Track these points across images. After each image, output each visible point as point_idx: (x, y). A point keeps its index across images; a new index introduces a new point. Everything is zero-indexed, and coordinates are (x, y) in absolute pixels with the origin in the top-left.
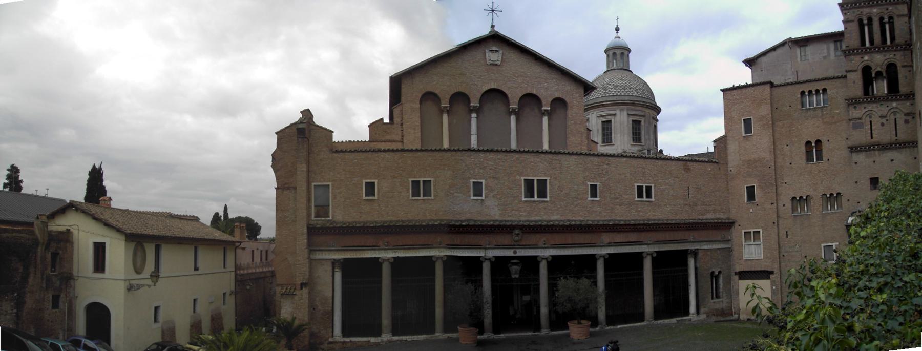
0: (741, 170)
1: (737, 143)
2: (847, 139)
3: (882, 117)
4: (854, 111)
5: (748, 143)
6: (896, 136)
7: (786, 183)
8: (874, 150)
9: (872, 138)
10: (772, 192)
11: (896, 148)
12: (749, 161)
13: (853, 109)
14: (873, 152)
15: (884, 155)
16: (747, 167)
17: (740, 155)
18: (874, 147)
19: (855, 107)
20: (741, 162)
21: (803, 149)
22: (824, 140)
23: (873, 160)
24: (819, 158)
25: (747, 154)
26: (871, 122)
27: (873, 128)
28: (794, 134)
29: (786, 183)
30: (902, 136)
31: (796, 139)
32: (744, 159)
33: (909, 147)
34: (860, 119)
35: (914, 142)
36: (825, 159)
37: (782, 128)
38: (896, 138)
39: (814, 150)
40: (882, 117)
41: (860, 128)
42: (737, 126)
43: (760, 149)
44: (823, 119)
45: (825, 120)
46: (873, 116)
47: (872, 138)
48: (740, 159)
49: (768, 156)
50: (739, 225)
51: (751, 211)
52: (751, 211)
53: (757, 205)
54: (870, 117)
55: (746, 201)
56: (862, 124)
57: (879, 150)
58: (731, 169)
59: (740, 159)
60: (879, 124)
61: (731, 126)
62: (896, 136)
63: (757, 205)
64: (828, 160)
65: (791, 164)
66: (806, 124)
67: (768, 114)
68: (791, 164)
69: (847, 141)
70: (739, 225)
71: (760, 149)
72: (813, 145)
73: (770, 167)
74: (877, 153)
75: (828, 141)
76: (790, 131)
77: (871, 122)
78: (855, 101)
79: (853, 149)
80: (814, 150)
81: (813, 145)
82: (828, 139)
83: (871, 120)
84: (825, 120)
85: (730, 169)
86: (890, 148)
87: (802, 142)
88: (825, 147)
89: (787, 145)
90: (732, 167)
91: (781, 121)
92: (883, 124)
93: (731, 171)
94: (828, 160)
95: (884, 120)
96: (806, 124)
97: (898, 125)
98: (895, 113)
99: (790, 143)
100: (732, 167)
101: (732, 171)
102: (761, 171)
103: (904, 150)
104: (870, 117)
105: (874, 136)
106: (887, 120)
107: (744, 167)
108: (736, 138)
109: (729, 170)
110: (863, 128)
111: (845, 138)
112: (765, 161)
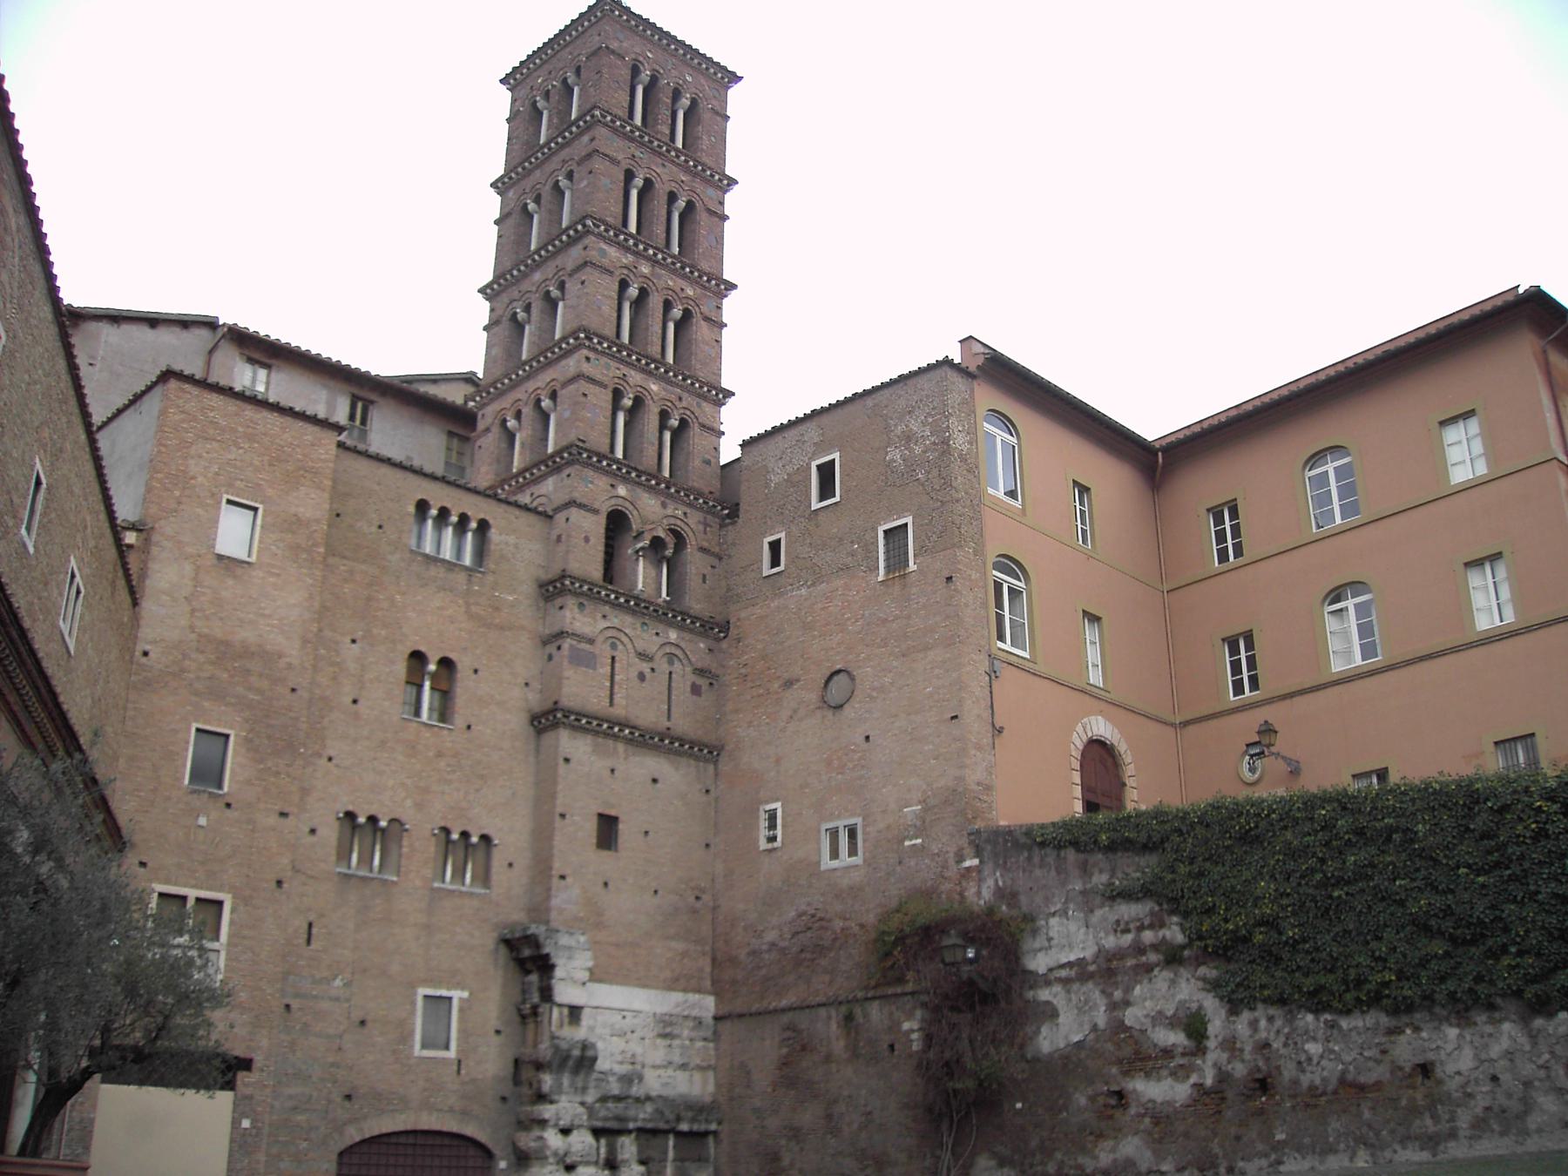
0: (187, 663)
1: (188, 568)
2: (527, 684)
3: (643, 656)
4: (577, 616)
5: (230, 582)
6: (669, 718)
7: (330, 759)
8: (615, 737)
9: (611, 703)
10: (289, 776)
11: (669, 752)
12: (227, 644)
13: (576, 610)
14: (610, 742)
15: (637, 759)
16: (213, 663)
17: (193, 611)
18: (620, 730)
19: (581, 605)
20: (193, 636)
21: (401, 668)
22: (463, 663)
23: (609, 763)
24: (444, 712)
25: (221, 619)
26: (613, 658)
27: (617, 678)
28: (379, 613)
29: (330, 759)
30: (682, 724)
31: (383, 632)
32: (206, 630)
33: (697, 759)
34: (591, 641)
35: (715, 747)
36: (459, 721)
37: (346, 580)
38: (668, 724)
39: (427, 684)
40: (643, 656)
41: (586, 667)
42: (200, 511)
43: (270, 616)
44: (468, 604)
45: (474, 609)
46: (620, 647)
47: (611, 703)
48: (192, 628)
49: (294, 652)
50: (143, 864)
51: (202, 821)
52: (202, 821)
53: (228, 805)
54: (614, 646)
55: (186, 782)
56: (594, 656)
57: (629, 741)
58: (147, 648)
59: (192, 628)
60: (634, 674)
61: (179, 503)
62: (669, 718)
63: (228, 805)
64: (469, 727)
65: (355, 702)
66: (419, 598)
67: (318, 521)
68: (355, 702)
69: (526, 689)
70: (143, 864)
71: (270, 616)
72: (432, 667)
73: (293, 690)
74: (621, 747)
75: (476, 671)
76: (369, 599)
77: (613, 658)
78: (590, 589)
79: (567, 717)
80: (427, 684)
81: (432, 667)
82: (477, 667)
83: (615, 654)
84: (474, 609)
85: (141, 647)
86: (655, 748)
87: (399, 647)
88: (465, 685)
89: (354, 641)
90: (154, 642)
91: (344, 557)
92: (642, 677)
93: (146, 654)
94: (469, 727)
95: (645, 667)
96: (419, 598)
97: (674, 692)
98: (671, 663)
99: (364, 637)
100: (150, 643)
101: (151, 654)
102: (260, 691)
103: (684, 760)
104: (614, 646)
105: (617, 698)
106: (653, 670)
107: (201, 658)
108: (189, 550)
109: (138, 654)
110: (595, 669)
111: (521, 681)
112: (282, 663)
